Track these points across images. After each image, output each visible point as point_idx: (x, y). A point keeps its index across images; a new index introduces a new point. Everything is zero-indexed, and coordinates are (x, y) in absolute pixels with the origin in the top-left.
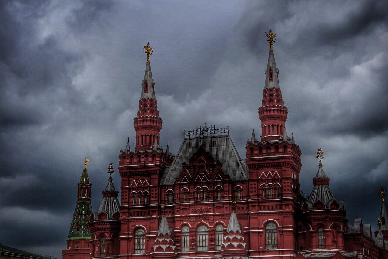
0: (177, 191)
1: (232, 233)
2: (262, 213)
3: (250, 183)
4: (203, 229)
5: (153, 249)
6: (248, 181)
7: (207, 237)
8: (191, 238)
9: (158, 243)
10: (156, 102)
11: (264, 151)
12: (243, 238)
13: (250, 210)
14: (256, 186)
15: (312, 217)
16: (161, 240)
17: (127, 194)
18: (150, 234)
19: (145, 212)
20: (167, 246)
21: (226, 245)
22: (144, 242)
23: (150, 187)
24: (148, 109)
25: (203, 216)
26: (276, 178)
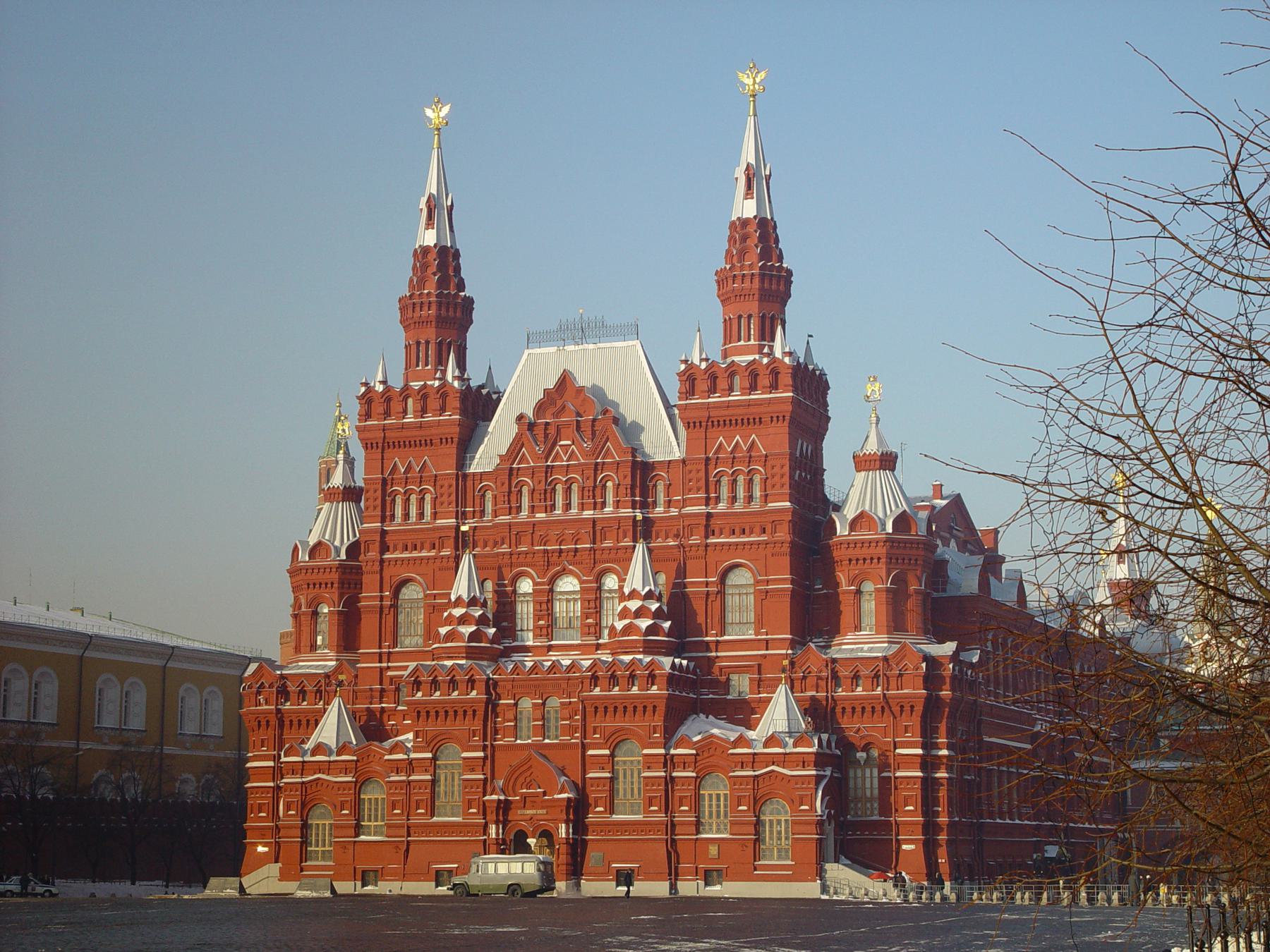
1: (633, 594)
2: (716, 545)
4: (568, 584)
6: (684, 461)
10: (457, 255)
11: (722, 384)
12: (665, 608)
14: (702, 474)
16: (458, 612)
17: (379, 493)
18: (435, 596)
20: (473, 628)
21: (619, 625)
24: (435, 274)
25: (568, 551)
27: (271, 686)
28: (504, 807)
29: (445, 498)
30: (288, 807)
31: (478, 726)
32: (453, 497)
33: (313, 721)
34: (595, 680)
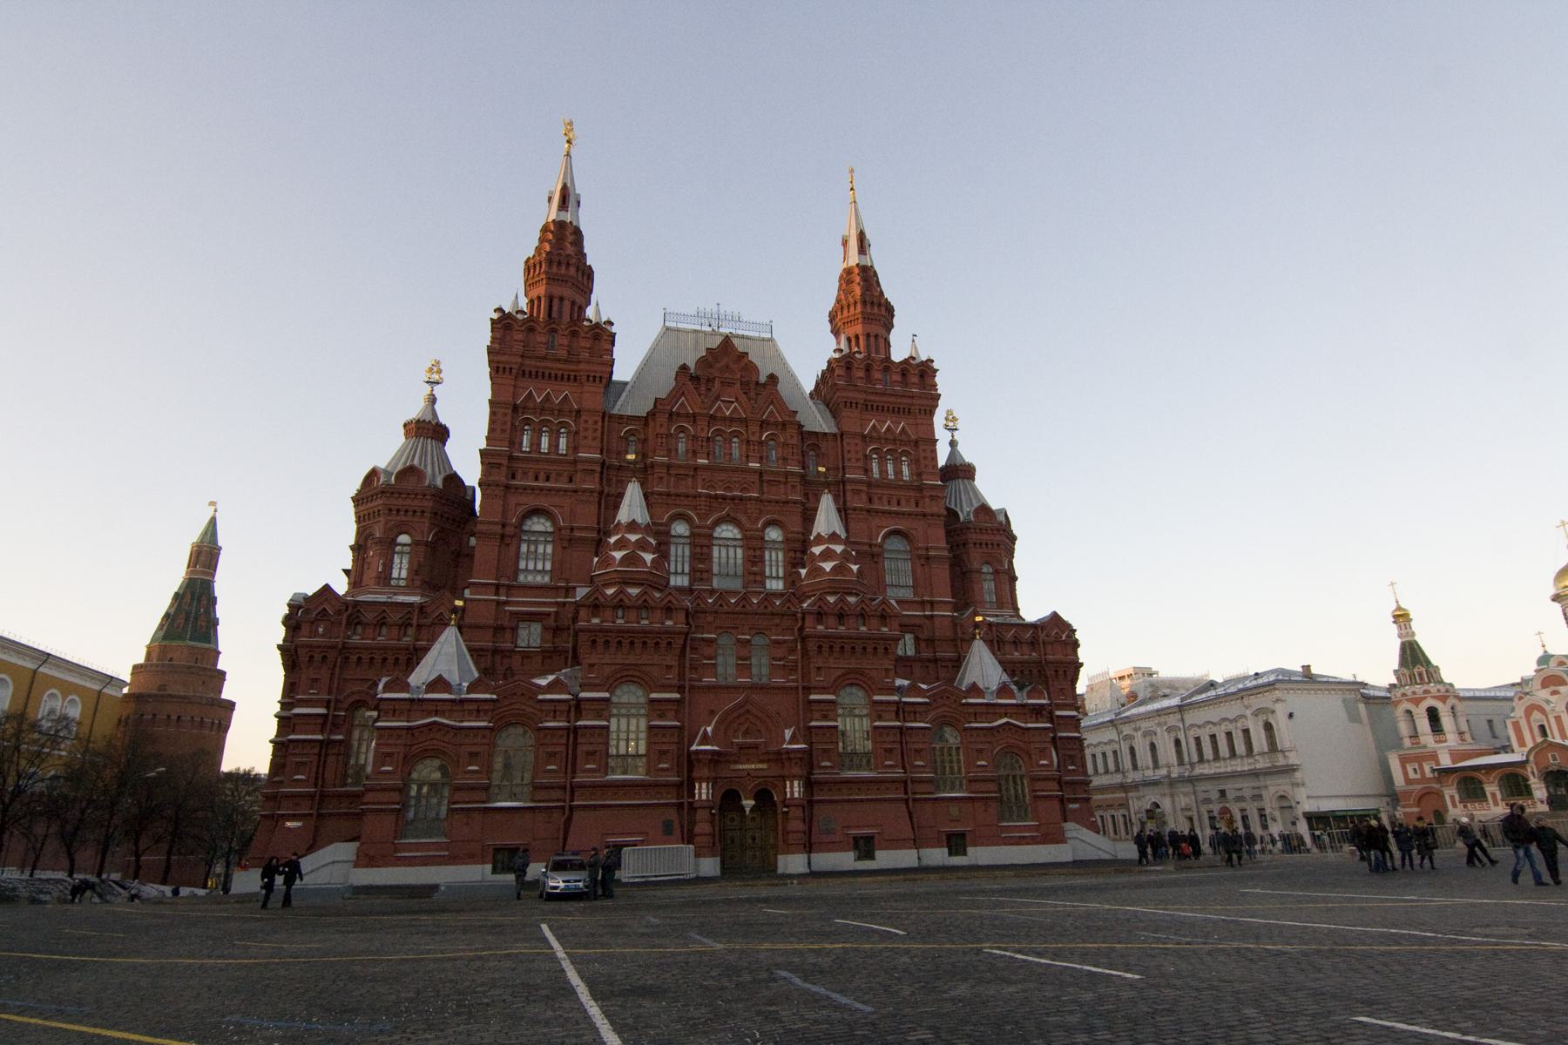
0: (663, 430)
1: (834, 537)
2: (877, 511)
3: (846, 441)
4: (727, 531)
5: (607, 561)
7: (739, 551)
8: (698, 550)
9: (620, 545)
13: (849, 498)
15: (973, 537)
16: (633, 538)
17: (509, 418)
19: (559, 475)
22: (549, 549)
23: (578, 412)
25: (733, 498)
26: (904, 437)
27: (339, 612)
28: (715, 759)
29: (590, 433)
30: (382, 758)
31: (671, 660)
32: (599, 434)
33: (414, 656)
34: (820, 616)
